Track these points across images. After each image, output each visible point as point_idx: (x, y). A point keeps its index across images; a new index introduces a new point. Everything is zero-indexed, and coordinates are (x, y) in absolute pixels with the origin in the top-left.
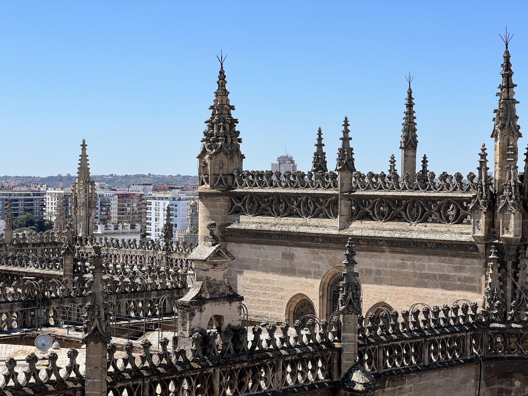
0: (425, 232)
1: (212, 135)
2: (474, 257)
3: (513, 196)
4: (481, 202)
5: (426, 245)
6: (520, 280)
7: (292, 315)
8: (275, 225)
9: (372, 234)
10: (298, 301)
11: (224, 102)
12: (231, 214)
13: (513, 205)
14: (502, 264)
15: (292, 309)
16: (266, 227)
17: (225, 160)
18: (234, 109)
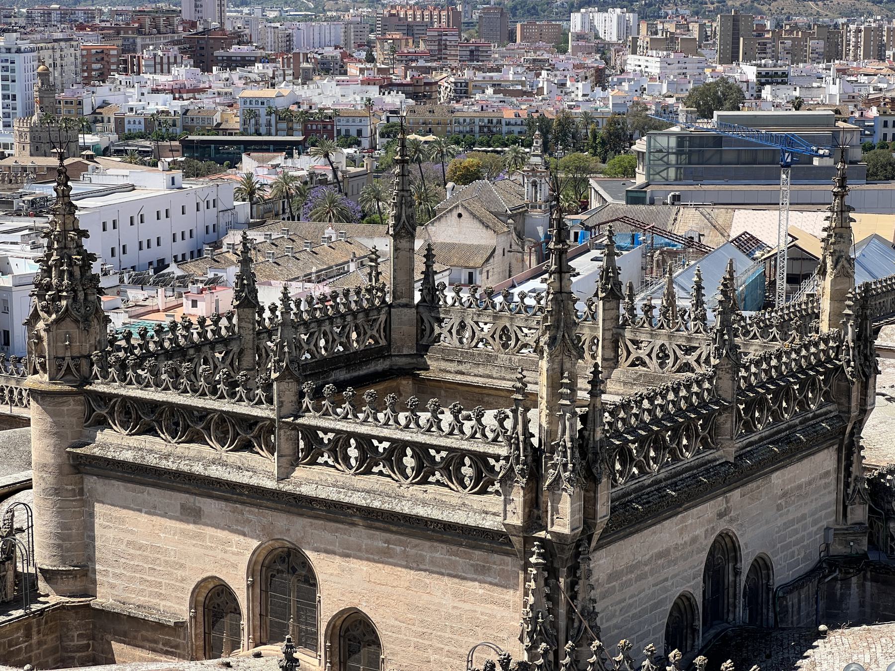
0: (425, 503)
1: (49, 287)
2: (507, 554)
3: (570, 466)
4: (517, 468)
5: (426, 525)
6: (580, 597)
7: (201, 609)
8: (167, 457)
9: (333, 495)
10: (211, 586)
11: (69, 226)
12: (89, 426)
13: (569, 480)
14: (550, 571)
15: (201, 599)
16: (151, 460)
17: (75, 332)
18: (87, 237)
